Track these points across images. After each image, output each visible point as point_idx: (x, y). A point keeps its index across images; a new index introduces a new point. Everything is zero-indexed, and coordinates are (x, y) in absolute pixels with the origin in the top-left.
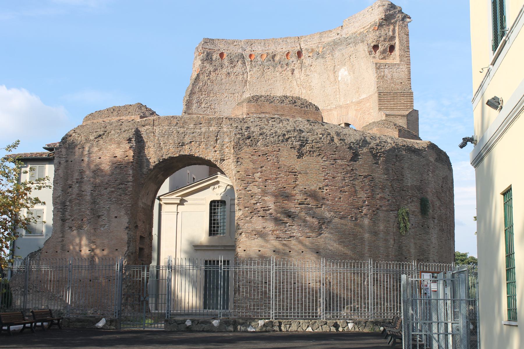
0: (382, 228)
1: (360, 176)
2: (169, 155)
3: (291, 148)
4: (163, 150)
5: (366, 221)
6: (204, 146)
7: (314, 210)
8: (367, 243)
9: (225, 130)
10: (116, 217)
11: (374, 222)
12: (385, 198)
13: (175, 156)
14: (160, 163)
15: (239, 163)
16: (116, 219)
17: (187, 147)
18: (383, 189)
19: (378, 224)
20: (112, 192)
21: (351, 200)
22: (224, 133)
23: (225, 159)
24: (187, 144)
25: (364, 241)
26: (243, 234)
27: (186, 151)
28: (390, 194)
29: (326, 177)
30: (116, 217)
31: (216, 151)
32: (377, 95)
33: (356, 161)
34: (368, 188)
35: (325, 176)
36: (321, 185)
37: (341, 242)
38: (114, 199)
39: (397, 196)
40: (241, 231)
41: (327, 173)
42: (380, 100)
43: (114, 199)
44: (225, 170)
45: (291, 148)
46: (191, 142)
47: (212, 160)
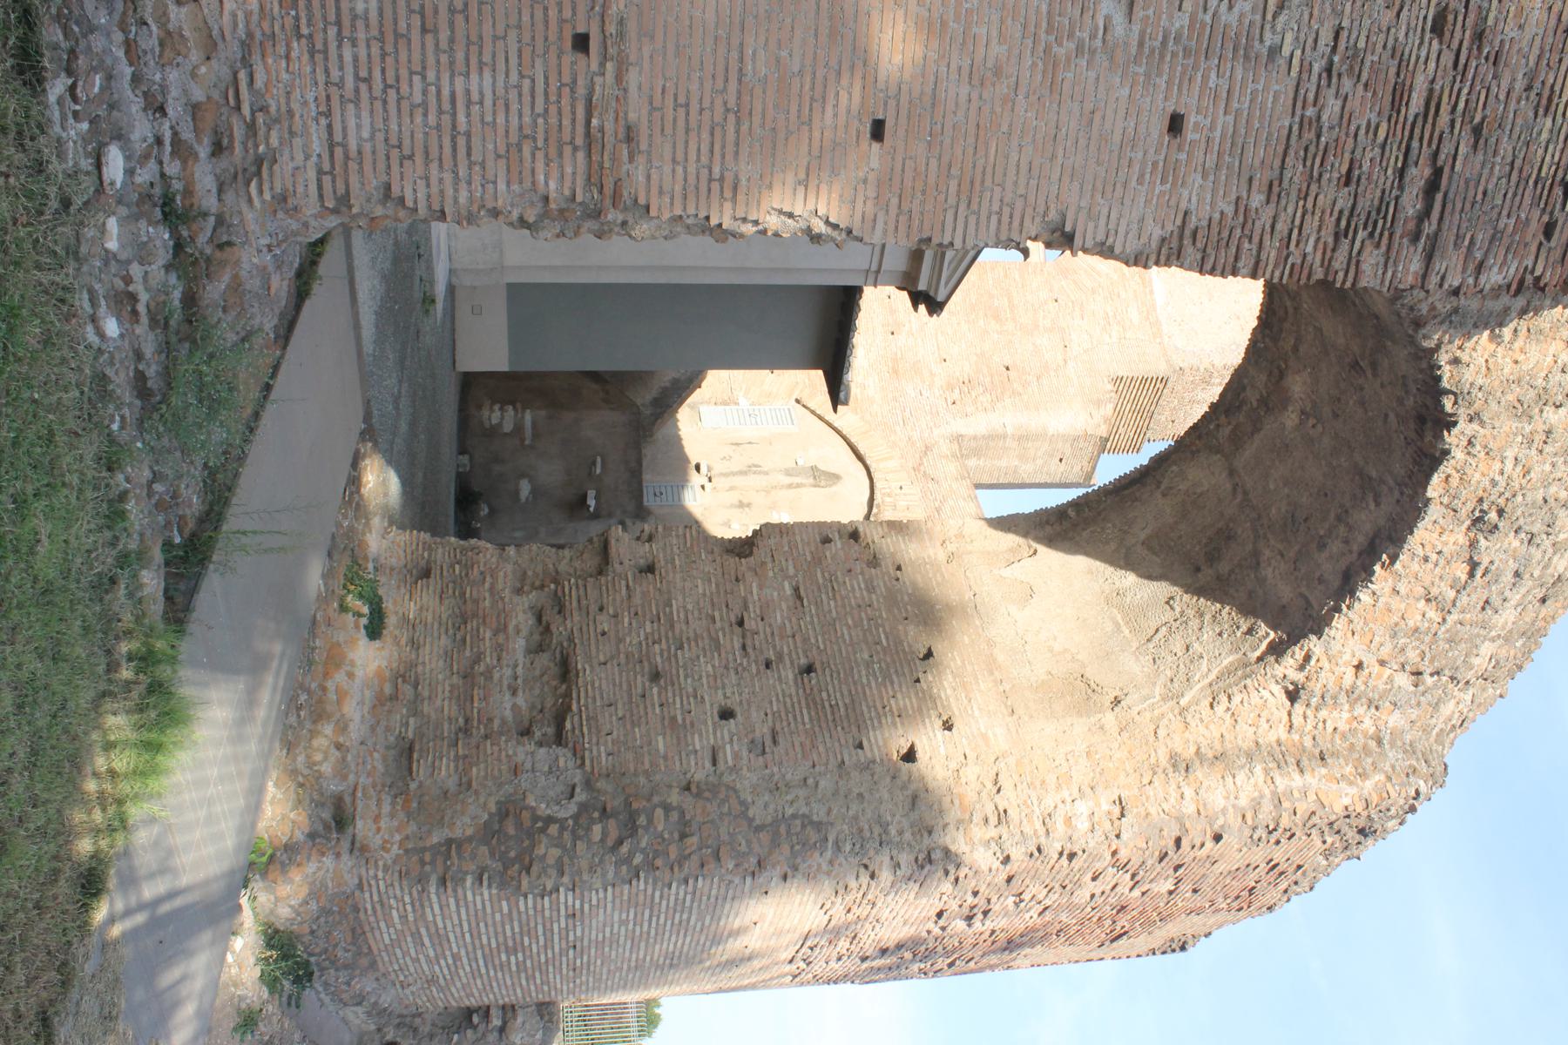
2: (1458, 454)
4: (1508, 425)
6: (1414, 620)
9: (1448, 709)
10: (1175, 124)
13: (1436, 479)
14: (1432, 388)
15: (1261, 832)
16: (1159, 125)
17: (1458, 538)
20: (1399, 96)
22: (1436, 706)
23: (1299, 708)
24: (1473, 544)
26: (865, 879)
27: (1436, 535)
30: (1175, 124)
31: (1359, 667)
32: (1161, 369)
38: (1332, 107)
40: (886, 876)
42: (1144, 380)
43: (1332, 107)
44: (1237, 699)
46: (1473, 565)
47: (1313, 643)
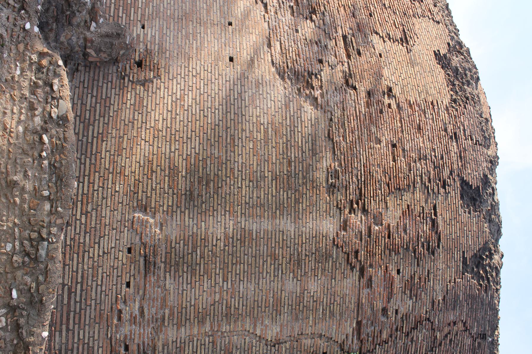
0: (314, 286)
1: (435, 208)
3: (449, 44)
5: (329, 226)
7: (339, 67)
8: (266, 225)
11: (328, 256)
12: (389, 302)
18: (412, 288)
19: (324, 270)
21: (378, 174)
25: (274, 217)
28: (400, 316)
29: (417, 109)
33: (462, 197)
34: (412, 232)
35: (419, 106)
36: (396, 91)
37: (266, 131)
39: (395, 344)
41: (425, 113)
45: (449, 44)
